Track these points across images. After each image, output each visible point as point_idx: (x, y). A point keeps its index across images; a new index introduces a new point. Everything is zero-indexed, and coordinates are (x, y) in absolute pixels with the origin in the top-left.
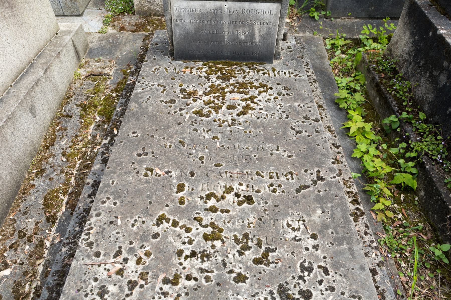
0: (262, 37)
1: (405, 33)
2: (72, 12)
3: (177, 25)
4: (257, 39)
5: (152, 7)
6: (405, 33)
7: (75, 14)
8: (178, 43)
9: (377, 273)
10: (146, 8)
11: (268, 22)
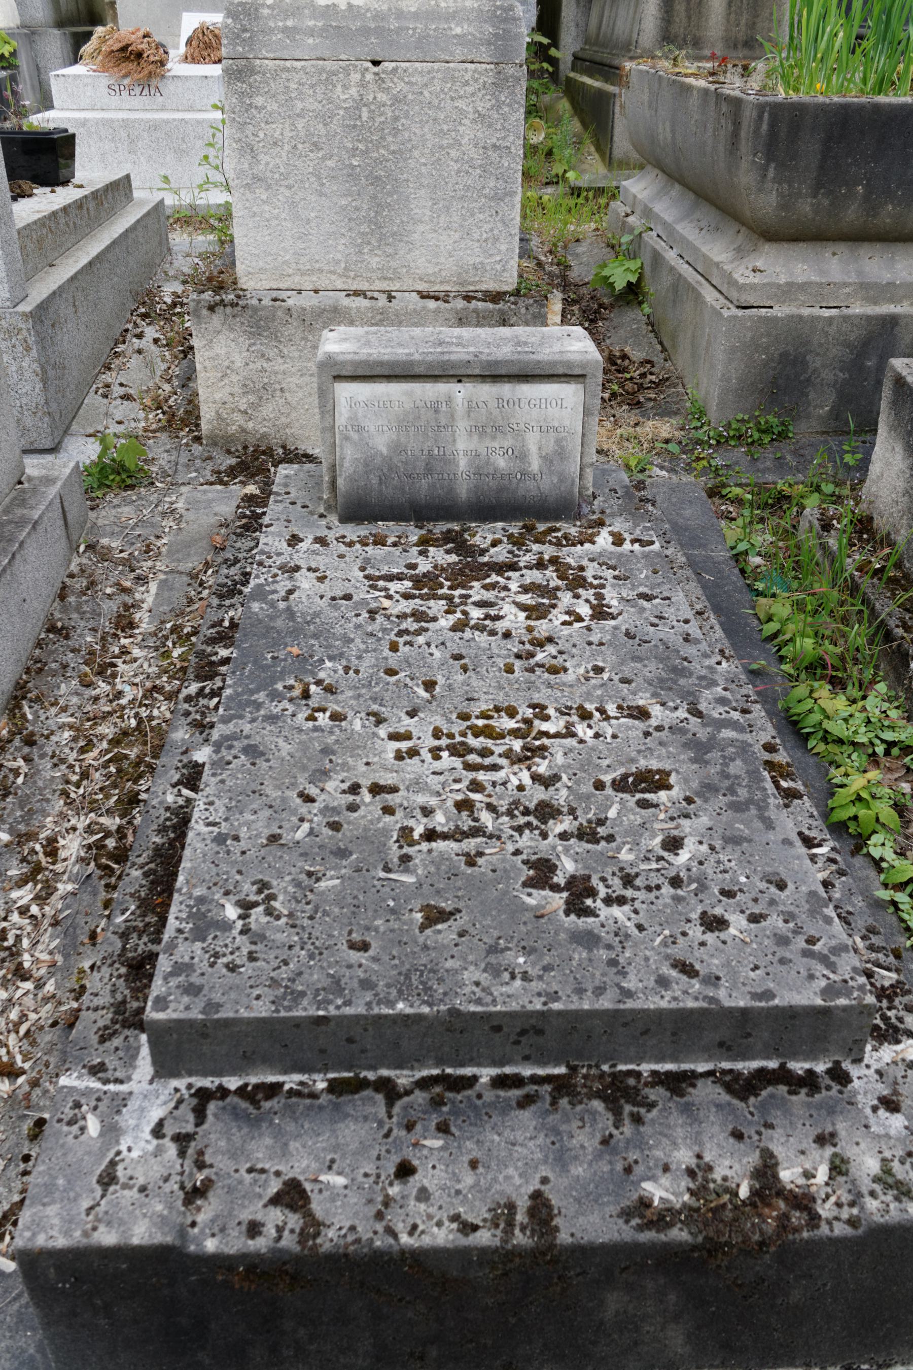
0: (547, 459)
1: (893, 449)
2: (32, 443)
3: (347, 438)
4: (535, 465)
5: (251, 425)
6: (893, 449)
7: (41, 447)
8: (351, 479)
9: (833, 886)
10: (234, 428)
11: (556, 425)
